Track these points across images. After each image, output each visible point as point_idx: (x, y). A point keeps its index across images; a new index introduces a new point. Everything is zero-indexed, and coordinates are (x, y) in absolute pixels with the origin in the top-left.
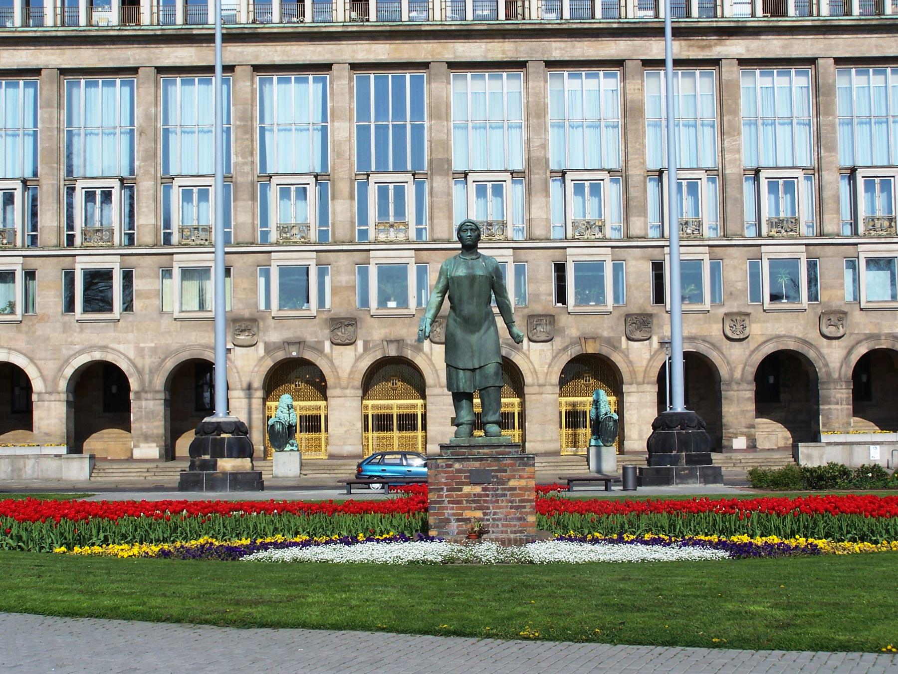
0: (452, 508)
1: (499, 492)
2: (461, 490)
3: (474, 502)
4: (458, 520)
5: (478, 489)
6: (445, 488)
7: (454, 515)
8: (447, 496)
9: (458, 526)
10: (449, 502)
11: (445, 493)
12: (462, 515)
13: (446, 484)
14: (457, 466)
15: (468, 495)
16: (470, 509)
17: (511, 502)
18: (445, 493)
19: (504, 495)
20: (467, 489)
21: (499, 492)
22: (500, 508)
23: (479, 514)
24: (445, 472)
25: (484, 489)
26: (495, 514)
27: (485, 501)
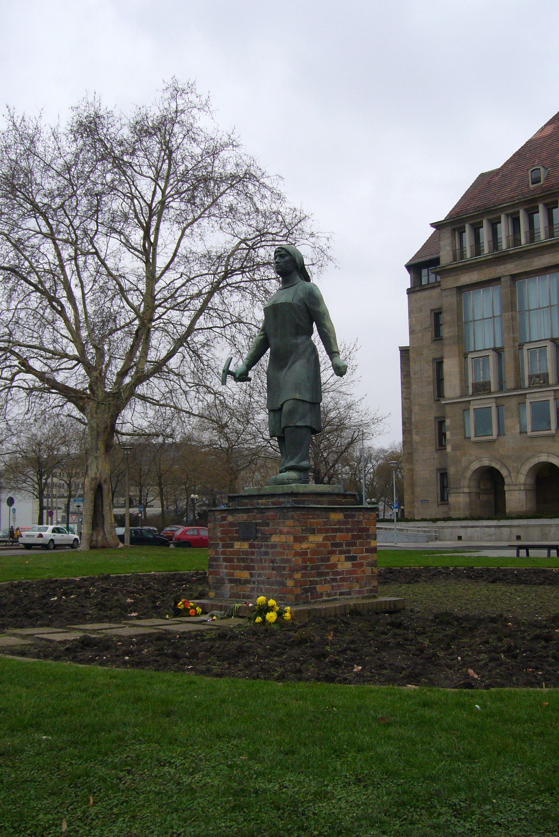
0: (226, 567)
1: (263, 549)
2: (232, 546)
3: (243, 560)
4: (231, 581)
5: (245, 546)
6: (221, 544)
7: (228, 574)
8: (223, 553)
9: (232, 588)
10: (225, 560)
11: (220, 549)
12: (233, 575)
13: (222, 539)
14: (230, 518)
15: (238, 552)
16: (239, 568)
17: (273, 561)
18: (220, 549)
19: (266, 553)
20: (237, 545)
21: (263, 549)
22: (263, 568)
23: (245, 575)
24: (222, 526)
25: (251, 546)
26: (260, 575)
27: (252, 560)
